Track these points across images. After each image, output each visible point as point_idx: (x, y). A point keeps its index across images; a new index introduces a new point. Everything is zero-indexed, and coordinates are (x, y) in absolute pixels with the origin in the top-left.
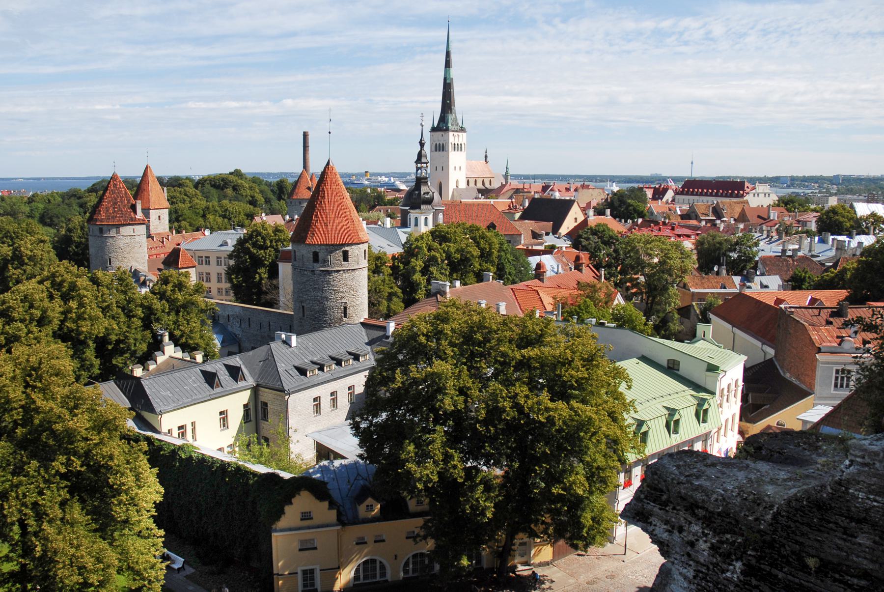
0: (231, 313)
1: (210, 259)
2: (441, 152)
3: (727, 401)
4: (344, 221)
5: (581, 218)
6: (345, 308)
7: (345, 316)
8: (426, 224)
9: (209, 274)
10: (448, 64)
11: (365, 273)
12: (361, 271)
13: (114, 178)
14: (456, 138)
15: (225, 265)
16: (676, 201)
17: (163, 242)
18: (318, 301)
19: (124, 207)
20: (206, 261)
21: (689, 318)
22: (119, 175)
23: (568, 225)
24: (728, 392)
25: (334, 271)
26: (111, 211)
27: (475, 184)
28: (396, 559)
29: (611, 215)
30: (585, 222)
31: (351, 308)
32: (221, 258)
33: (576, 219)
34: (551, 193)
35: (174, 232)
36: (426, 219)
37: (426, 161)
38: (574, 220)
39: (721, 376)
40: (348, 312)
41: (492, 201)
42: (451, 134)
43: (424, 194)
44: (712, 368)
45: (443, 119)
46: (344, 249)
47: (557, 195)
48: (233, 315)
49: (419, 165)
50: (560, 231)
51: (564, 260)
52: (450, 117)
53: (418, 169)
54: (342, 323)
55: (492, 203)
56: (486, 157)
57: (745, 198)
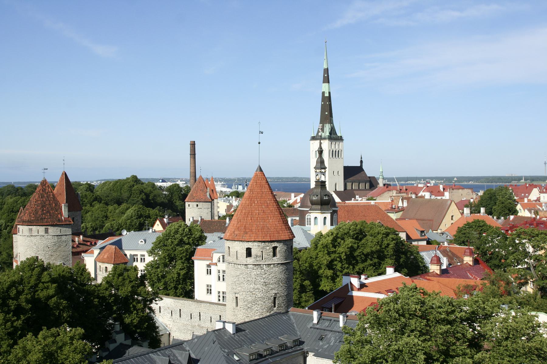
7: (275, 306)
8: (325, 224)
10: (326, 80)
13: (44, 183)
15: (141, 261)
16: (542, 200)
18: (251, 292)
19: (52, 209)
22: (48, 180)
25: (266, 265)
26: (40, 213)
29: (486, 212)
32: (137, 255)
33: (452, 216)
36: (325, 218)
37: (323, 167)
41: (372, 202)
46: (274, 246)
49: (318, 171)
51: (450, 254)
55: (374, 204)
56: (361, 162)
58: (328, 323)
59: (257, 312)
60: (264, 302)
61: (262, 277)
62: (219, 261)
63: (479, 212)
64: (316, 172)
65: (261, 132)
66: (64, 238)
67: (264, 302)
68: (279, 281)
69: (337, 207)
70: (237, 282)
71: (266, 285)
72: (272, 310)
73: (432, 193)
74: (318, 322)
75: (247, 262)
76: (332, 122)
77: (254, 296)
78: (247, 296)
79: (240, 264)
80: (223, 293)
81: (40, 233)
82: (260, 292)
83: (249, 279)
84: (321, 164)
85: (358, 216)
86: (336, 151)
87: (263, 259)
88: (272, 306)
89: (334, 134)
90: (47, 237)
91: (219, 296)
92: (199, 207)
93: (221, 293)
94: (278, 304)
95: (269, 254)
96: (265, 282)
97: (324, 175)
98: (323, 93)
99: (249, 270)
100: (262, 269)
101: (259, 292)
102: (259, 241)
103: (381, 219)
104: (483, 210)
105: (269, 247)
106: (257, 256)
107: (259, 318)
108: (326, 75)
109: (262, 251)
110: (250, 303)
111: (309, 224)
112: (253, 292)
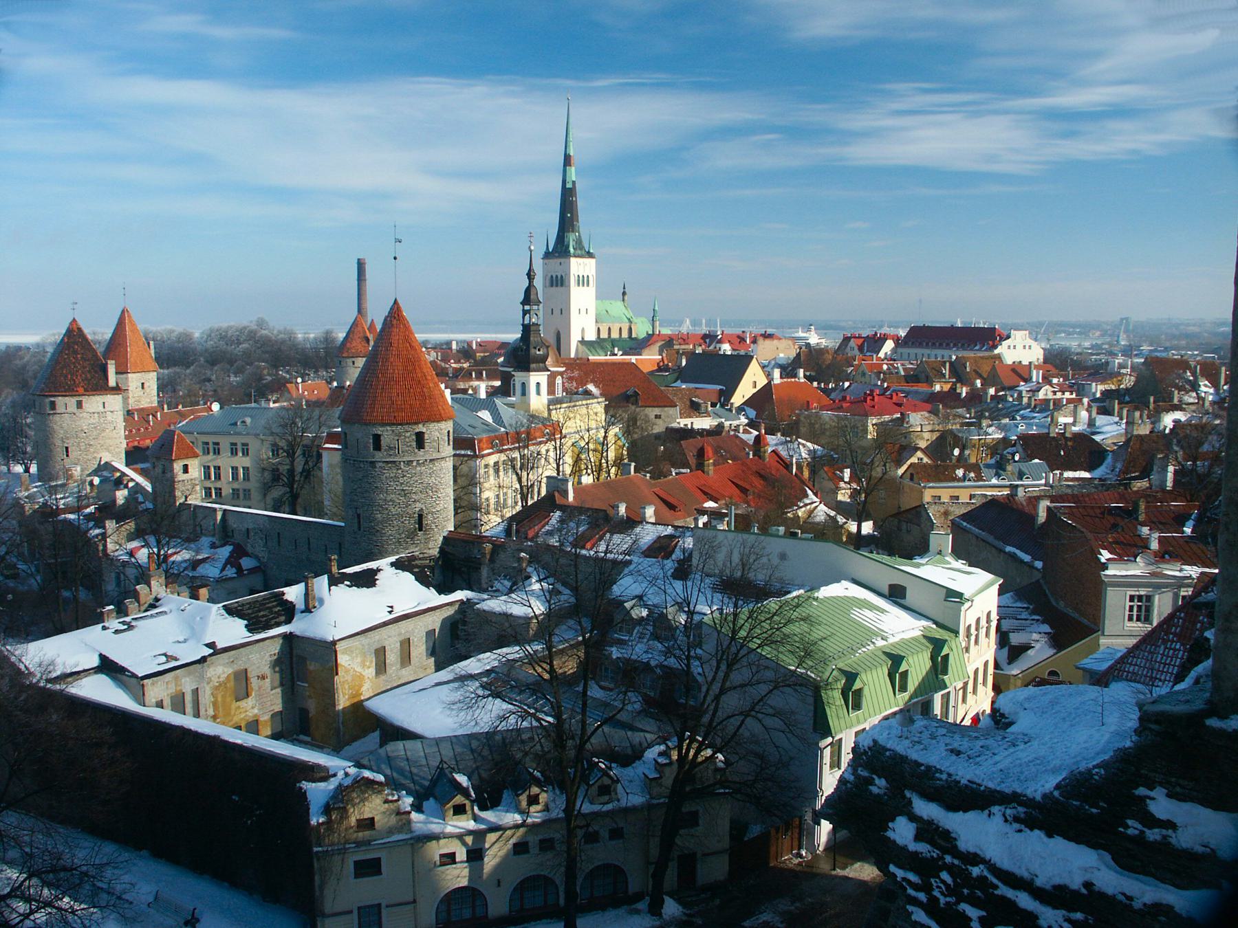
0: (251, 526)
1: (221, 446)
2: (559, 289)
3: (976, 642)
5: (762, 381)
6: (421, 516)
8: (538, 393)
9: (219, 468)
11: (449, 465)
14: (581, 267)
17: (148, 422)
20: (214, 449)
21: (919, 526)
23: (744, 391)
24: (977, 629)
27: (609, 334)
28: (499, 882)
30: (768, 388)
31: (430, 516)
32: (236, 444)
33: (755, 382)
34: (718, 346)
35: (166, 406)
38: (752, 385)
39: (963, 608)
40: (425, 522)
41: (633, 359)
42: (573, 260)
44: (953, 595)
45: (561, 239)
46: (417, 430)
47: (726, 348)
48: (254, 529)
49: (527, 307)
50: (732, 401)
52: (571, 238)
53: (525, 313)
55: (634, 361)
56: (624, 294)
57: (996, 352)
63: (795, 376)
64: (523, 310)
66: (109, 417)
70: (359, 490)
77: (386, 512)
81: (69, 410)
84: (528, 298)
90: (81, 415)
92: (356, 365)
100: (398, 469)
102: (394, 424)
104: (801, 372)
105: (409, 434)
106: (390, 447)
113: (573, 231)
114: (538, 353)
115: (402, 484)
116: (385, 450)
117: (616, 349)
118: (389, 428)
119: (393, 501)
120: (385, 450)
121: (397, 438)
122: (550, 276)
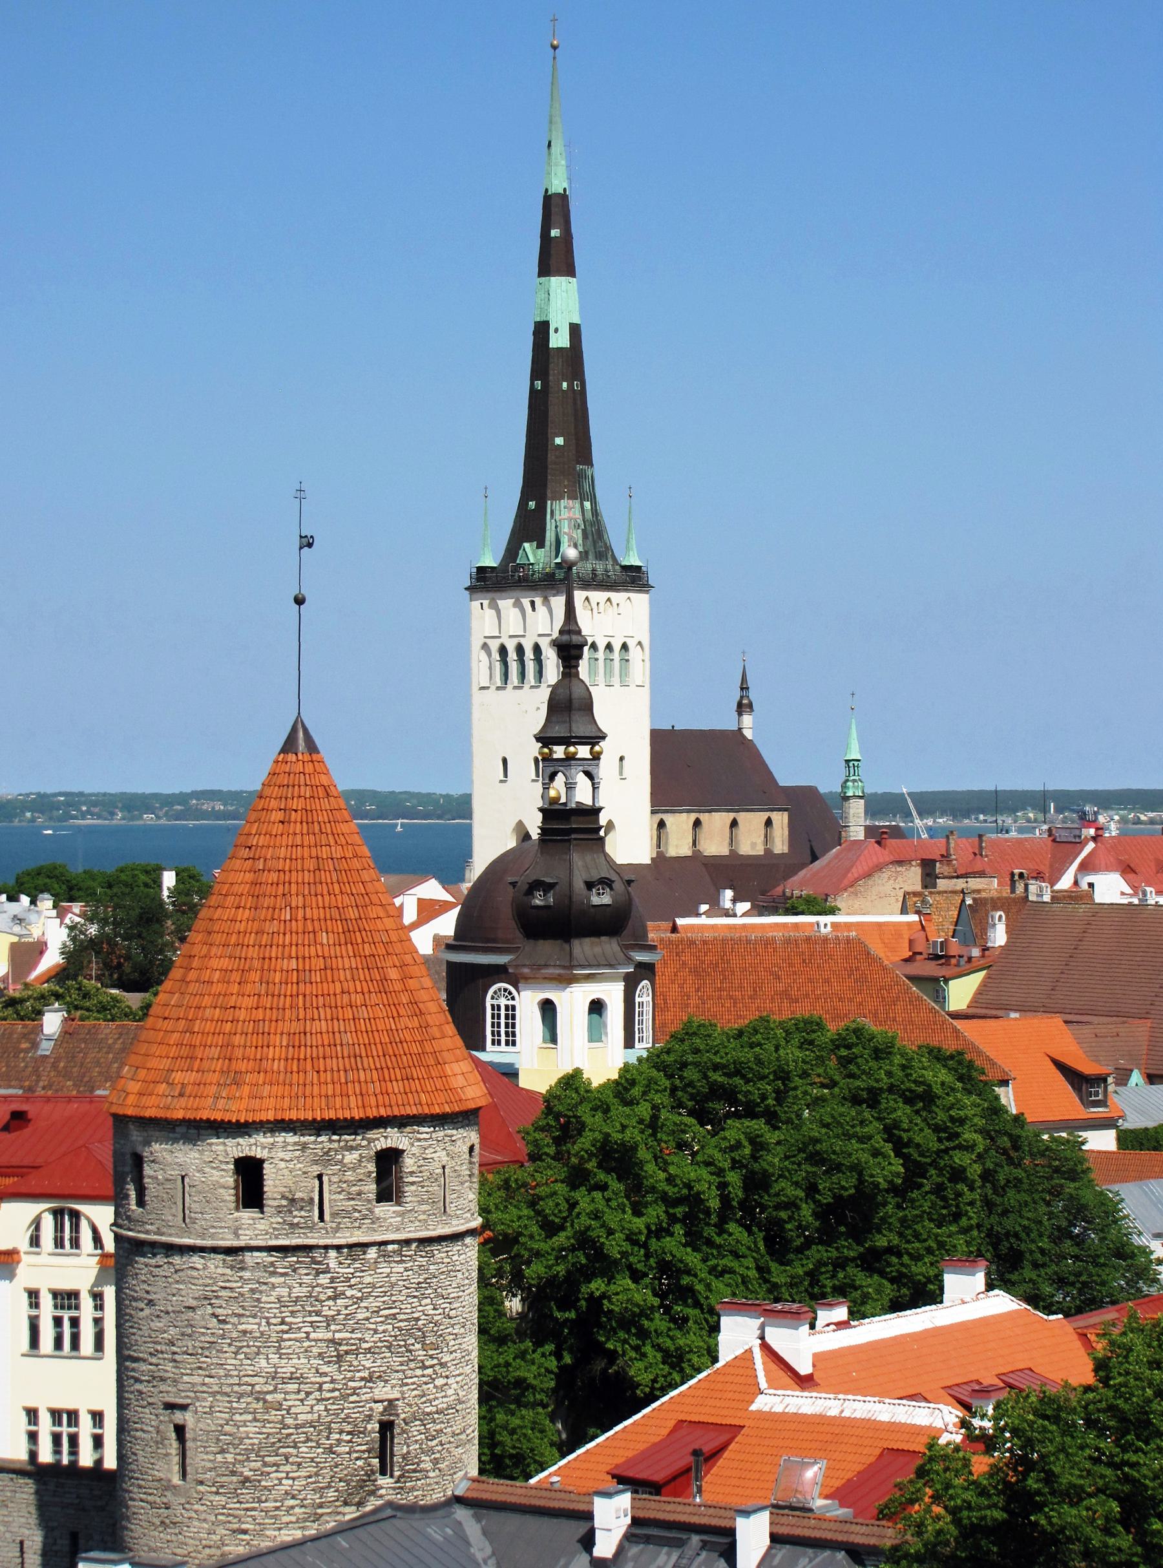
4: (380, 1012)
8: (596, 1034)
11: (469, 1254)
12: (456, 1247)
18: (260, 1397)
25: (338, 1248)
31: (415, 1428)
36: (597, 1007)
40: (400, 1449)
43: (590, 885)
46: (382, 1144)
49: (559, 752)
53: (548, 768)
54: (372, 1504)
56: (743, 707)
58: (669, 1555)
59: (292, 1502)
60: (330, 1450)
61: (318, 1313)
62: (35, 1241)
65: (305, 541)
67: (330, 1450)
68: (411, 1335)
69: (652, 948)
70: (180, 1343)
71: (339, 1356)
72: (372, 1493)
73: (1128, 870)
74: (620, 1551)
75: (237, 1236)
76: (586, 487)
78: (237, 1417)
79: (202, 1249)
80: (56, 1414)
82: (308, 1394)
83: (250, 1325)
85: (751, 997)
86: (609, 647)
87: (327, 1217)
88: (373, 1472)
89: (600, 556)
91: (33, 1437)
93: (45, 1420)
94: (404, 1457)
95: (354, 1188)
96: (332, 1341)
97: (589, 775)
98: (542, 330)
99: (247, 1274)
100: (318, 1273)
101: (302, 1395)
103: (875, 1015)
106: (293, 1201)
107: (298, 1534)
108: (555, 233)
109: (320, 1177)
110: (253, 1456)
111: (503, 1038)
112: (269, 1397)
113: (572, 497)
114: (596, 900)
115: (329, 1321)
116: (279, 1210)
117: (729, 894)
118: (291, 1138)
119: (300, 1379)
120: (279, 1210)
121: (316, 1170)
122: (494, 646)
